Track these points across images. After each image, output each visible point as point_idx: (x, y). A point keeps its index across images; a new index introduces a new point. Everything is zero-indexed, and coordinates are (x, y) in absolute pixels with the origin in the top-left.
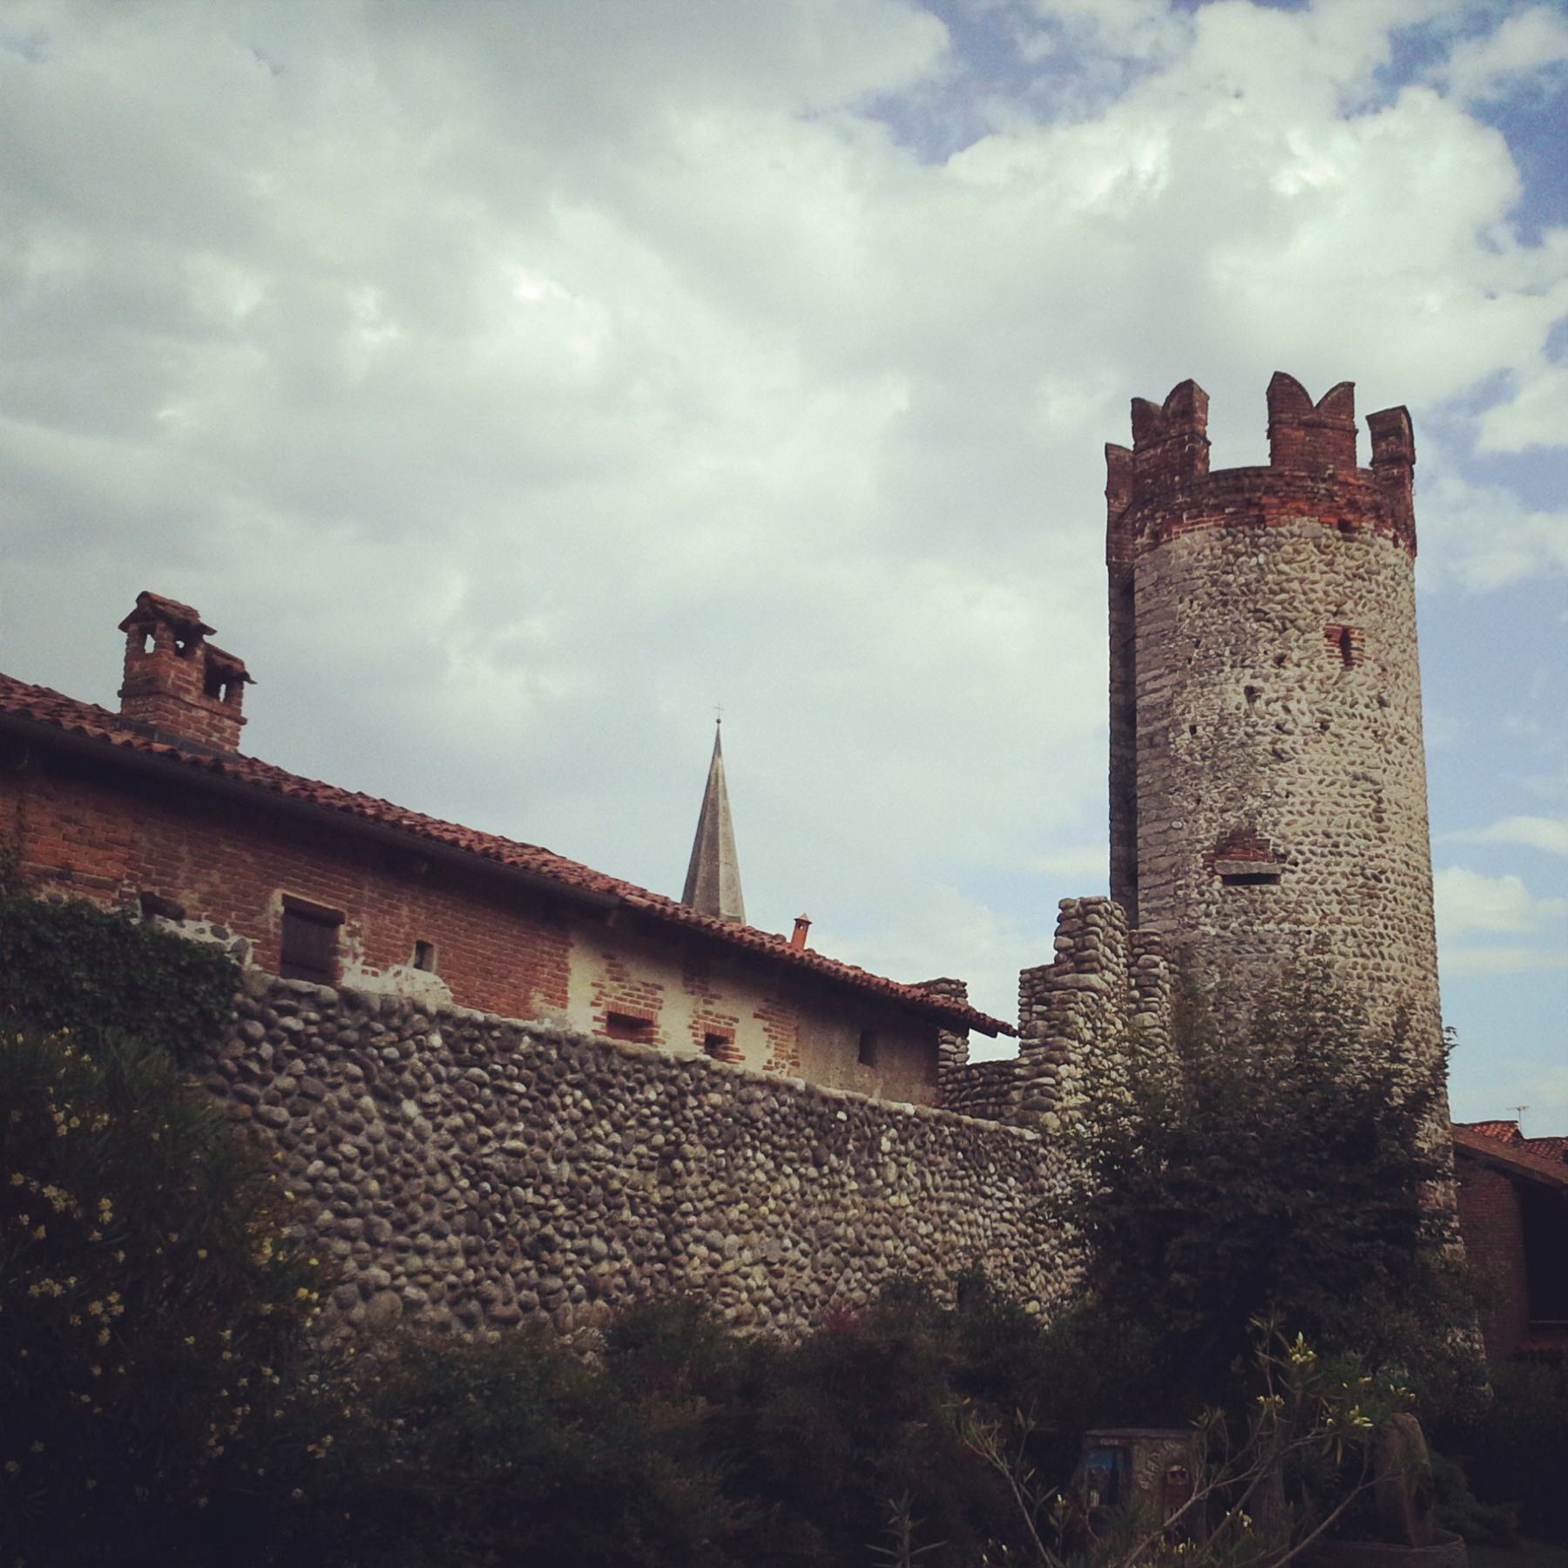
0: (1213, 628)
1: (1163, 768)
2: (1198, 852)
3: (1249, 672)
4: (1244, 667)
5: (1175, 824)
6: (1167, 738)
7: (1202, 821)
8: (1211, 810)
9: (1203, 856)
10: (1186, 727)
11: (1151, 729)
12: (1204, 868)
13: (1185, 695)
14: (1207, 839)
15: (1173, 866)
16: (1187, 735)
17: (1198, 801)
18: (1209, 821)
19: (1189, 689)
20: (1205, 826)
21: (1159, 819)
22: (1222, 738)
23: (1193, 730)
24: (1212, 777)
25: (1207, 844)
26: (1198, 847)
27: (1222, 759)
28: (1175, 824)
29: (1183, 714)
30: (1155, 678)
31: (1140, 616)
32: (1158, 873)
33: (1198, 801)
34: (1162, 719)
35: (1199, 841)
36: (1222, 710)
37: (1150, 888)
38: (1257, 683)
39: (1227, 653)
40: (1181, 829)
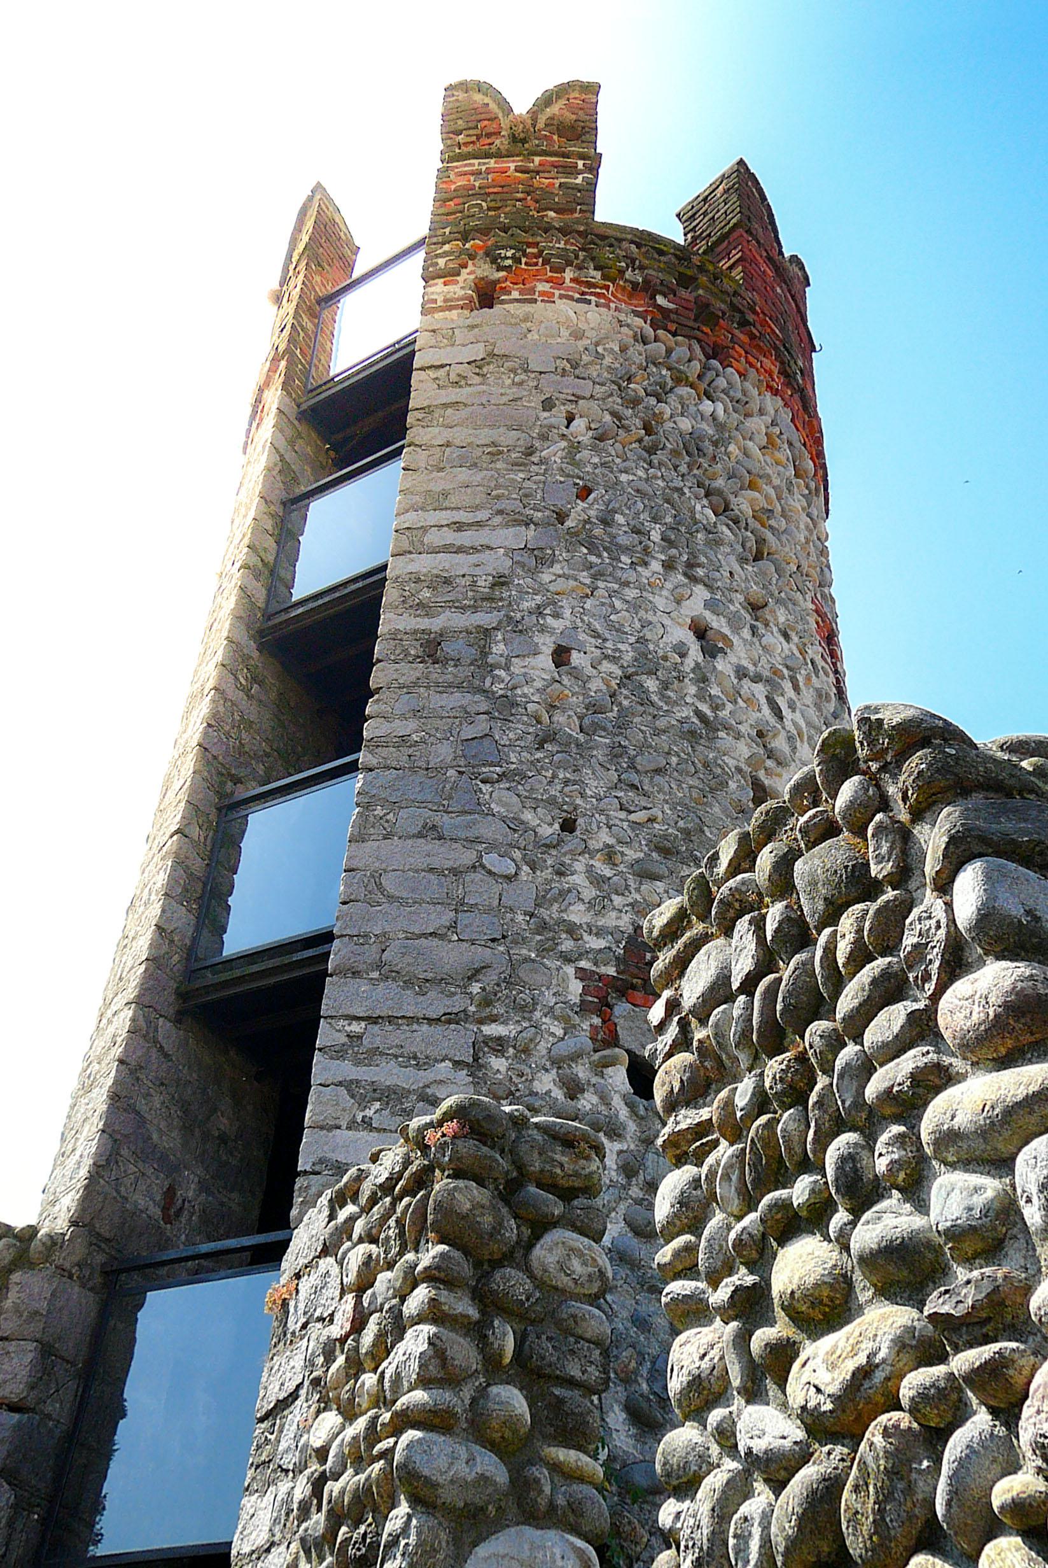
0: (624, 478)
1: (468, 716)
2: (567, 959)
3: (701, 593)
4: (694, 580)
5: (491, 860)
6: (485, 653)
7: (579, 879)
8: (610, 855)
9: (582, 974)
10: (547, 644)
11: (436, 624)
12: (584, 1008)
13: (546, 577)
14: (600, 933)
15: (474, 975)
16: (545, 661)
17: (568, 826)
18: (598, 881)
19: (557, 569)
20: (589, 893)
21: (430, 831)
22: (645, 700)
23: (561, 656)
24: (614, 776)
25: (595, 943)
26: (567, 945)
27: (643, 747)
28: (491, 860)
29: (539, 611)
30: (459, 527)
31: (427, 410)
32: (421, 984)
33: (568, 826)
34: (475, 609)
35: (572, 930)
36: (642, 640)
37: (373, 1020)
38: (718, 623)
39: (656, 536)
40: (509, 878)
